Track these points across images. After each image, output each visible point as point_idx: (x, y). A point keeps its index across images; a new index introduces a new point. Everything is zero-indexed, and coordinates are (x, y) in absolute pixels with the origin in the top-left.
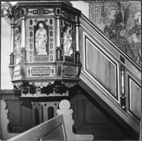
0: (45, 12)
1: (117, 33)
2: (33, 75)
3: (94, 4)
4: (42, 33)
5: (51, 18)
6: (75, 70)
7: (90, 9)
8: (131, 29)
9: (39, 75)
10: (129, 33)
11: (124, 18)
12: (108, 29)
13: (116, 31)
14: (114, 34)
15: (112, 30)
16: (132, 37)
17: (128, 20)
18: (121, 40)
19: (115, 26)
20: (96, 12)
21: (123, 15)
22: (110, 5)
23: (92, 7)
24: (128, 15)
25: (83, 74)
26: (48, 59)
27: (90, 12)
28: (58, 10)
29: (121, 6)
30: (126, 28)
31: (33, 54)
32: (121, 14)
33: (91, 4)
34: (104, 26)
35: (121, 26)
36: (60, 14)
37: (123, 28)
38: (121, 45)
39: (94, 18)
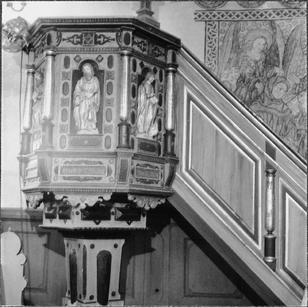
0: (98, 40)
1: (265, 91)
2: (65, 178)
3: (216, 25)
4: (90, 85)
5: (110, 55)
6: (163, 170)
7: (208, 36)
8: (298, 82)
9: (78, 179)
10: (294, 91)
11: (284, 57)
12: (246, 80)
13: (264, 87)
14: (260, 92)
15: (255, 83)
16: (300, 100)
17: (292, 61)
18: (273, 106)
19: (262, 74)
20: (221, 43)
21: (281, 50)
22: (253, 27)
23: (213, 31)
24: (292, 51)
25: (180, 179)
26: (98, 144)
27: (207, 43)
28: (127, 36)
29: (278, 29)
30: (286, 79)
31: (69, 133)
32: (277, 48)
33: (209, 24)
34: (237, 74)
35: (275, 75)
36: (130, 45)
37: (279, 80)
38: (274, 117)
39: (214, 56)
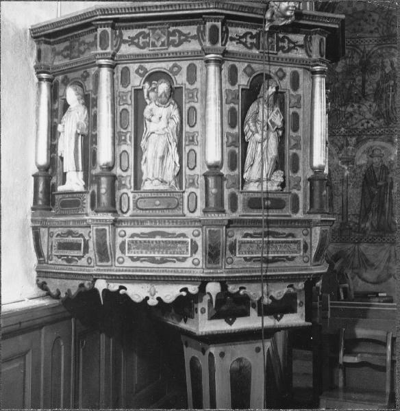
2: (132, 259)
6: (308, 237)
26: (179, 205)
28: (214, 28)
31: (132, 190)
36: (219, 45)
